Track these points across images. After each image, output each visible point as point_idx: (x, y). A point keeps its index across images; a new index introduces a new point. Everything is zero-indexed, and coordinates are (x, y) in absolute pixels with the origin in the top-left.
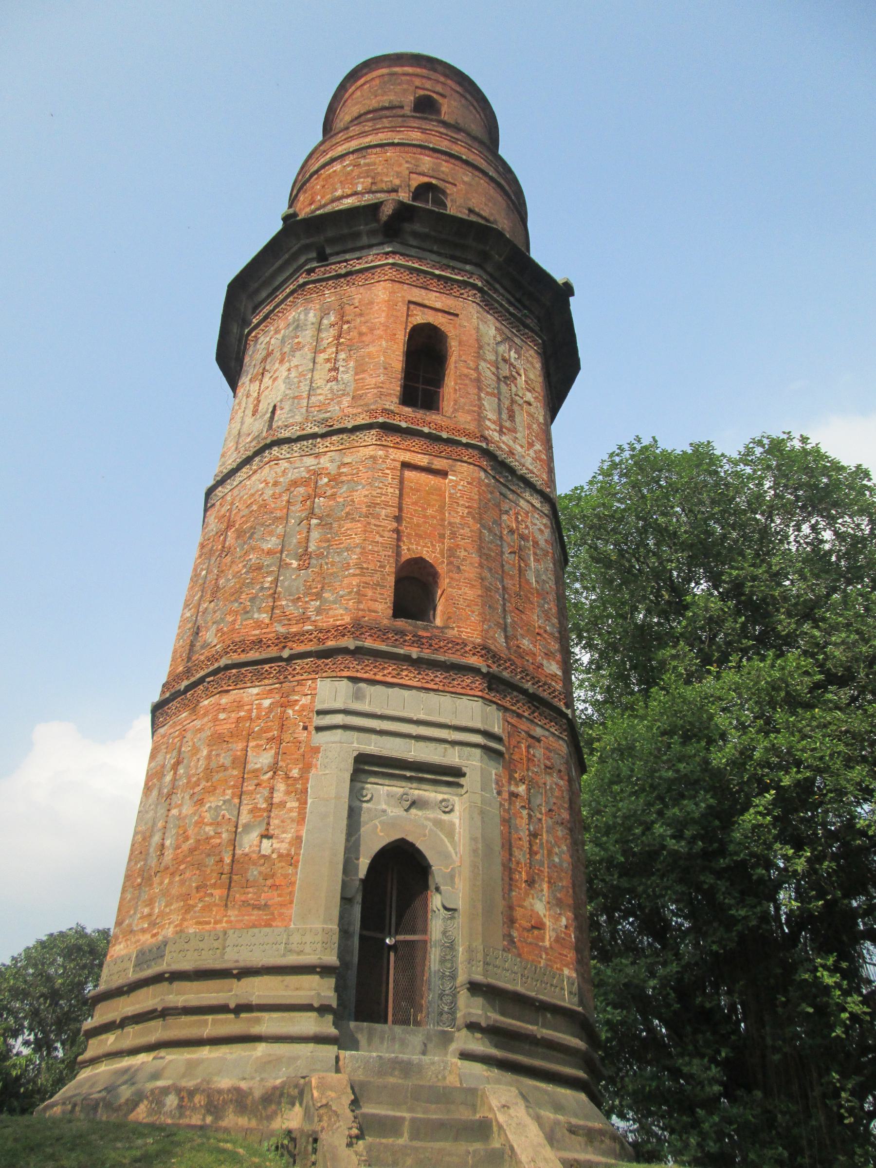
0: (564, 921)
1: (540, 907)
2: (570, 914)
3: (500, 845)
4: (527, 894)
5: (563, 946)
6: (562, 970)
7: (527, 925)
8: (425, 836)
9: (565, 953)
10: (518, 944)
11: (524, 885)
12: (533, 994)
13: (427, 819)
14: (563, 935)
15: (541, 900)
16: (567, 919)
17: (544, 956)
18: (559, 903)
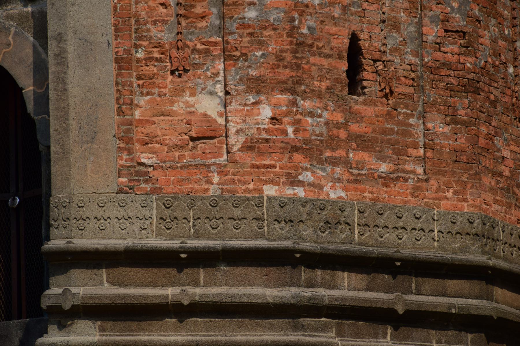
0: (266, 112)
1: (209, 106)
2: (284, 98)
3: (111, 30)
4: (178, 92)
5: (261, 154)
6: (261, 191)
7: (175, 140)
8: (9, 45)
9: (267, 162)
10: (156, 174)
11: (170, 78)
12: (175, 244)
13: (10, 17)
14: (264, 135)
15: (211, 93)
16: (276, 106)
17: (216, 179)
18: (257, 86)
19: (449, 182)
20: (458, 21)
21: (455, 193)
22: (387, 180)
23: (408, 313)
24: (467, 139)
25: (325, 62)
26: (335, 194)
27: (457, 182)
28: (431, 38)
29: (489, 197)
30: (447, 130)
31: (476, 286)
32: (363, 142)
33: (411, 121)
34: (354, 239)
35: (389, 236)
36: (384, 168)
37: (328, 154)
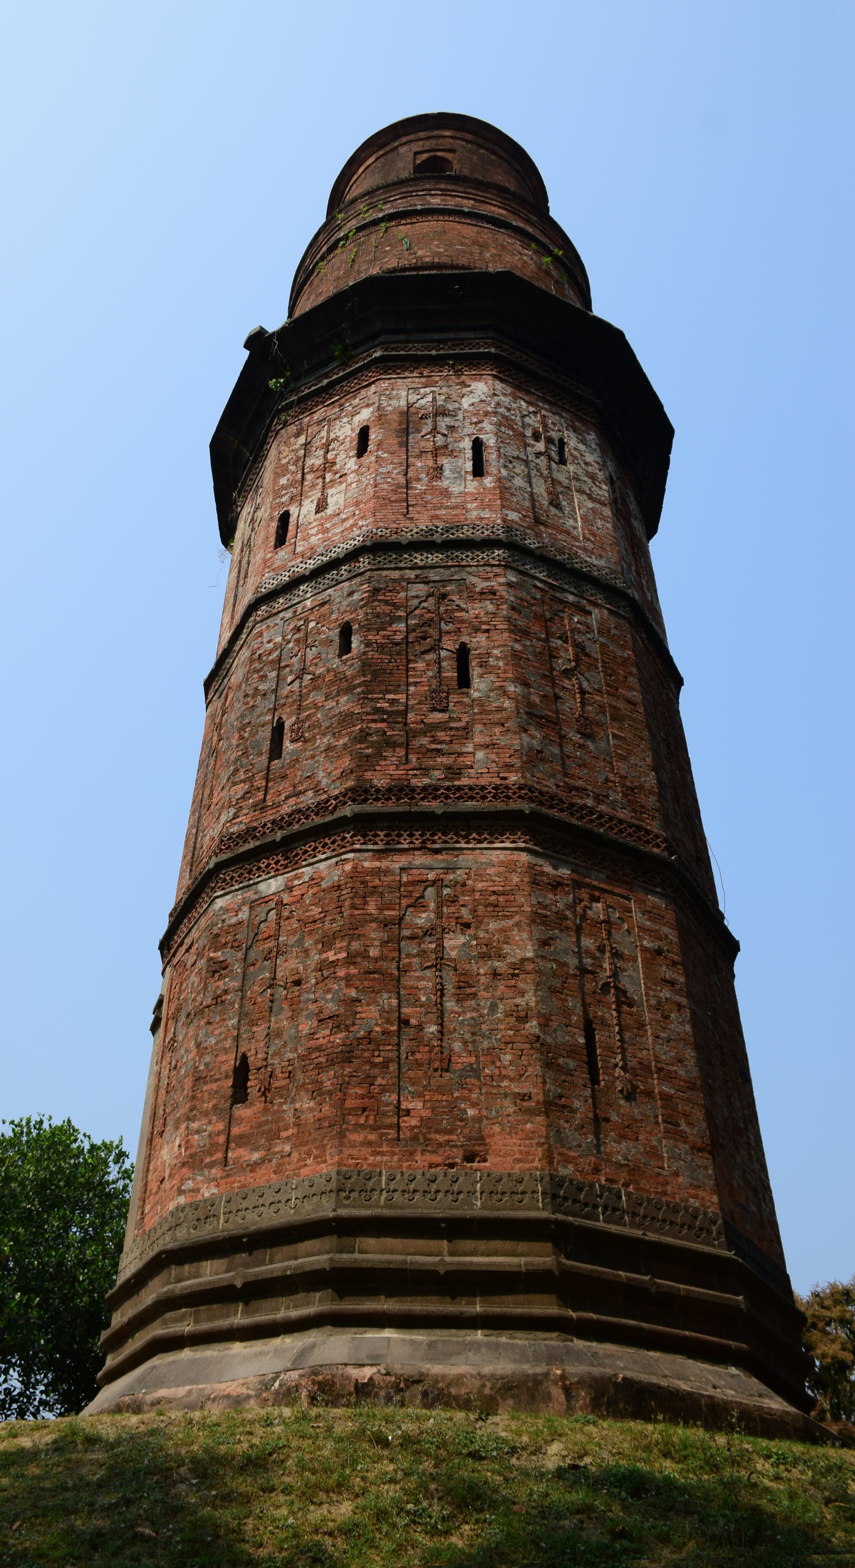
19: (310, 1150)
20: (331, 1007)
21: (316, 1157)
22: (254, 1167)
23: (246, 1285)
24: (331, 1106)
25: (214, 1086)
26: (207, 1192)
27: (317, 1148)
28: (305, 1032)
29: (366, 1151)
30: (312, 1104)
31: (328, 1242)
32: (244, 1140)
33: (284, 1107)
34: (220, 1227)
35: (252, 1216)
36: (256, 1156)
37: (207, 1160)
